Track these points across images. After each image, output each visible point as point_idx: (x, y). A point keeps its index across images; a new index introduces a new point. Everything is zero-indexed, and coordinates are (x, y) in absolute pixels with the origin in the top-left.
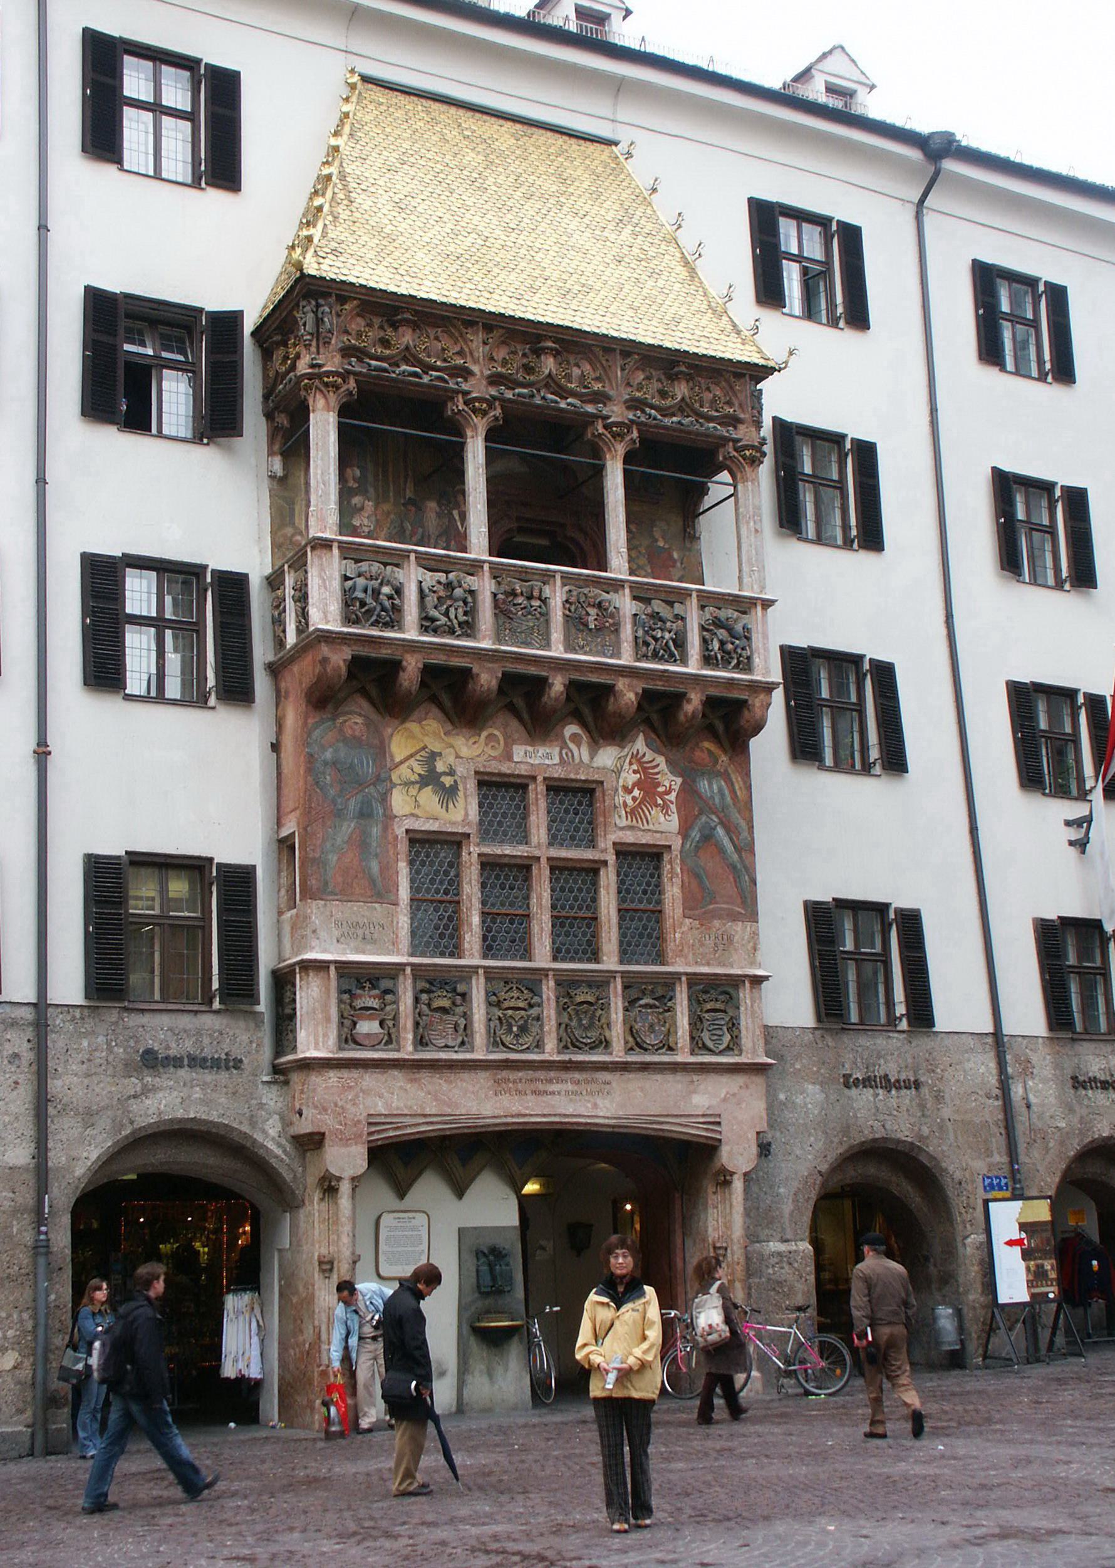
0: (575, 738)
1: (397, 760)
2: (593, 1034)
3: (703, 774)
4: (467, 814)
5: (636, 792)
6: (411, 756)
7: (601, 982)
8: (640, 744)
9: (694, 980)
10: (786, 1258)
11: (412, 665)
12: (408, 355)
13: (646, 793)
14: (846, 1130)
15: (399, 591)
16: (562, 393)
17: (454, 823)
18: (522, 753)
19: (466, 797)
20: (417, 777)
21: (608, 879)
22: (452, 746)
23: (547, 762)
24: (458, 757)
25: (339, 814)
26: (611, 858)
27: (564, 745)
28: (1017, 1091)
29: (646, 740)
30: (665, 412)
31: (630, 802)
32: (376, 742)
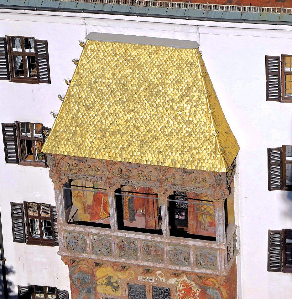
0: (160, 274)
1: (99, 277)
3: (210, 288)
4: (122, 294)
5: (183, 292)
6: (103, 277)
13: (187, 292)
15: (85, 241)
17: (118, 296)
18: (141, 278)
19: (122, 289)
20: (105, 283)
22: (117, 275)
23: (150, 281)
24: (118, 278)
25: (80, 291)
27: (156, 276)
29: (187, 277)
31: (181, 294)
32: (92, 273)
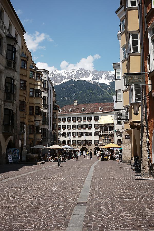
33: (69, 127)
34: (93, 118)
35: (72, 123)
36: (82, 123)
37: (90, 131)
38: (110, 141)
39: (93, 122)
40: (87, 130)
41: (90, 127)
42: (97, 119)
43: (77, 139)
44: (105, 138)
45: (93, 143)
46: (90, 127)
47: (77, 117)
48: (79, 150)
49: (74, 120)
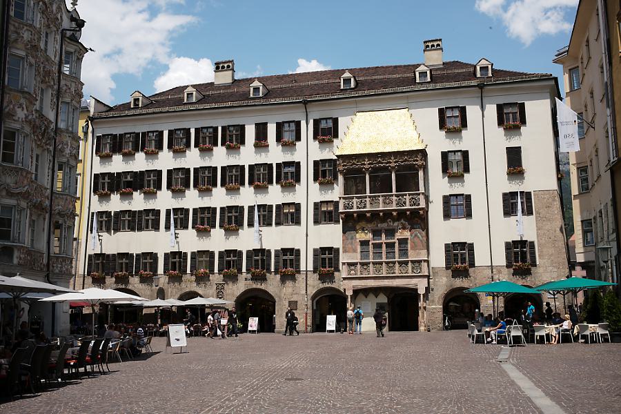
2: (392, 271)
7: (394, 263)
8: (402, 221)
9: (412, 262)
10: (436, 309)
11: (355, 215)
12: (354, 164)
14: (451, 286)
16: (382, 163)
21: (397, 245)
26: (396, 240)
28: (496, 277)
30: (402, 162)
33: (179, 180)
34: (307, 130)
35: (193, 159)
36: (248, 156)
37: (289, 198)
38: (404, 252)
39: (308, 151)
40: (275, 195)
41: (289, 175)
42: (327, 132)
43: (218, 241)
44: (376, 233)
45: (307, 262)
46: (289, 175)
47: (220, 123)
48: (229, 303)
49: (206, 141)
